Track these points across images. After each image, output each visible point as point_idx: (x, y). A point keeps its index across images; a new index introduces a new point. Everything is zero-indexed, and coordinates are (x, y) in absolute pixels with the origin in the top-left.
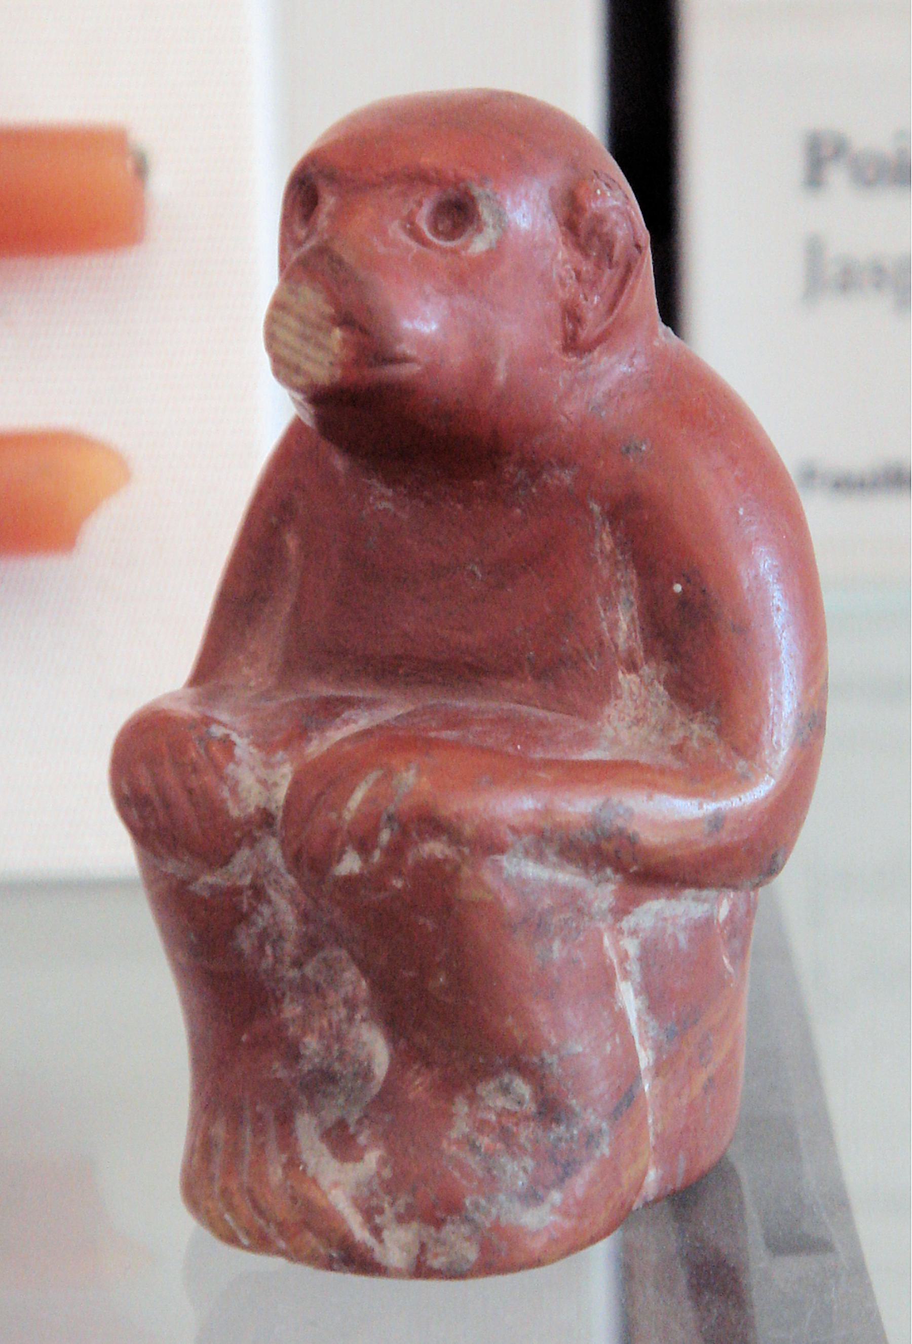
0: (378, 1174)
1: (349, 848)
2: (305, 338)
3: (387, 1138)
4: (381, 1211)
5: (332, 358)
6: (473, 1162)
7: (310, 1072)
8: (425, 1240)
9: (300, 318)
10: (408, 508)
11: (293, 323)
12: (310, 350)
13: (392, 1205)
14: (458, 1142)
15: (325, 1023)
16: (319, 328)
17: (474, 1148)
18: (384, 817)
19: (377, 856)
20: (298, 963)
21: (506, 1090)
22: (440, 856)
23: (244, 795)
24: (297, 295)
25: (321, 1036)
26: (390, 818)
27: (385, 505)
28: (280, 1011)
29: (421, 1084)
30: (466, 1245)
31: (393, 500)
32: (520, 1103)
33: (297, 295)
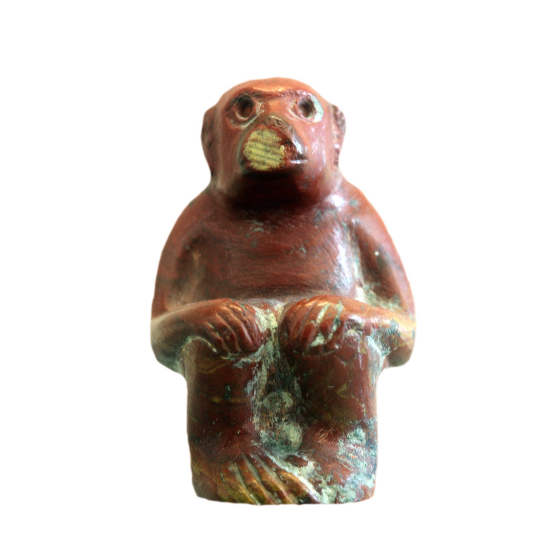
0: (316, 469)
1: (319, 334)
2: (267, 151)
3: (314, 457)
4: (320, 482)
5: (281, 157)
6: (349, 462)
7: (265, 443)
8: (339, 491)
9: (265, 144)
10: (270, 229)
11: (261, 146)
12: (269, 155)
13: (325, 479)
14: (342, 456)
15: (268, 425)
16: (274, 146)
17: (348, 458)
18: (335, 320)
19: (331, 336)
20: (262, 399)
21: (356, 435)
22: (353, 335)
23: (262, 323)
24: (262, 135)
25: (267, 430)
26: (337, 321)
27: (258, 229)
28: (252, 420)
29: (324, 436)
30: (352, 492)
31: (263, 227)
32: (361, 441)
33: (262, 135)
